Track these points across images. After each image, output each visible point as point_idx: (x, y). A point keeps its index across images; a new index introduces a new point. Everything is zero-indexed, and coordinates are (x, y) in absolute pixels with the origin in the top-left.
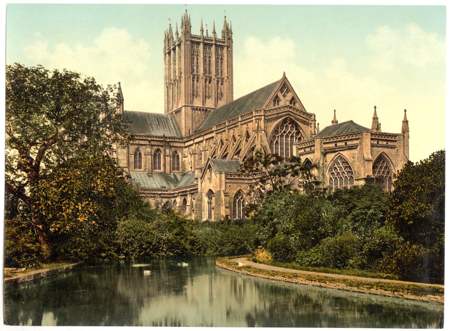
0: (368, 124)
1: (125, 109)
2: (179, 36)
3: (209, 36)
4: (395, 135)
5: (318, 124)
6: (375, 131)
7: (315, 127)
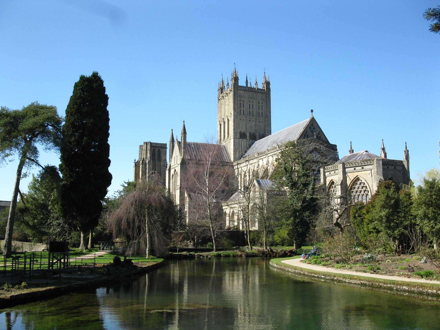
3: (252, 87)
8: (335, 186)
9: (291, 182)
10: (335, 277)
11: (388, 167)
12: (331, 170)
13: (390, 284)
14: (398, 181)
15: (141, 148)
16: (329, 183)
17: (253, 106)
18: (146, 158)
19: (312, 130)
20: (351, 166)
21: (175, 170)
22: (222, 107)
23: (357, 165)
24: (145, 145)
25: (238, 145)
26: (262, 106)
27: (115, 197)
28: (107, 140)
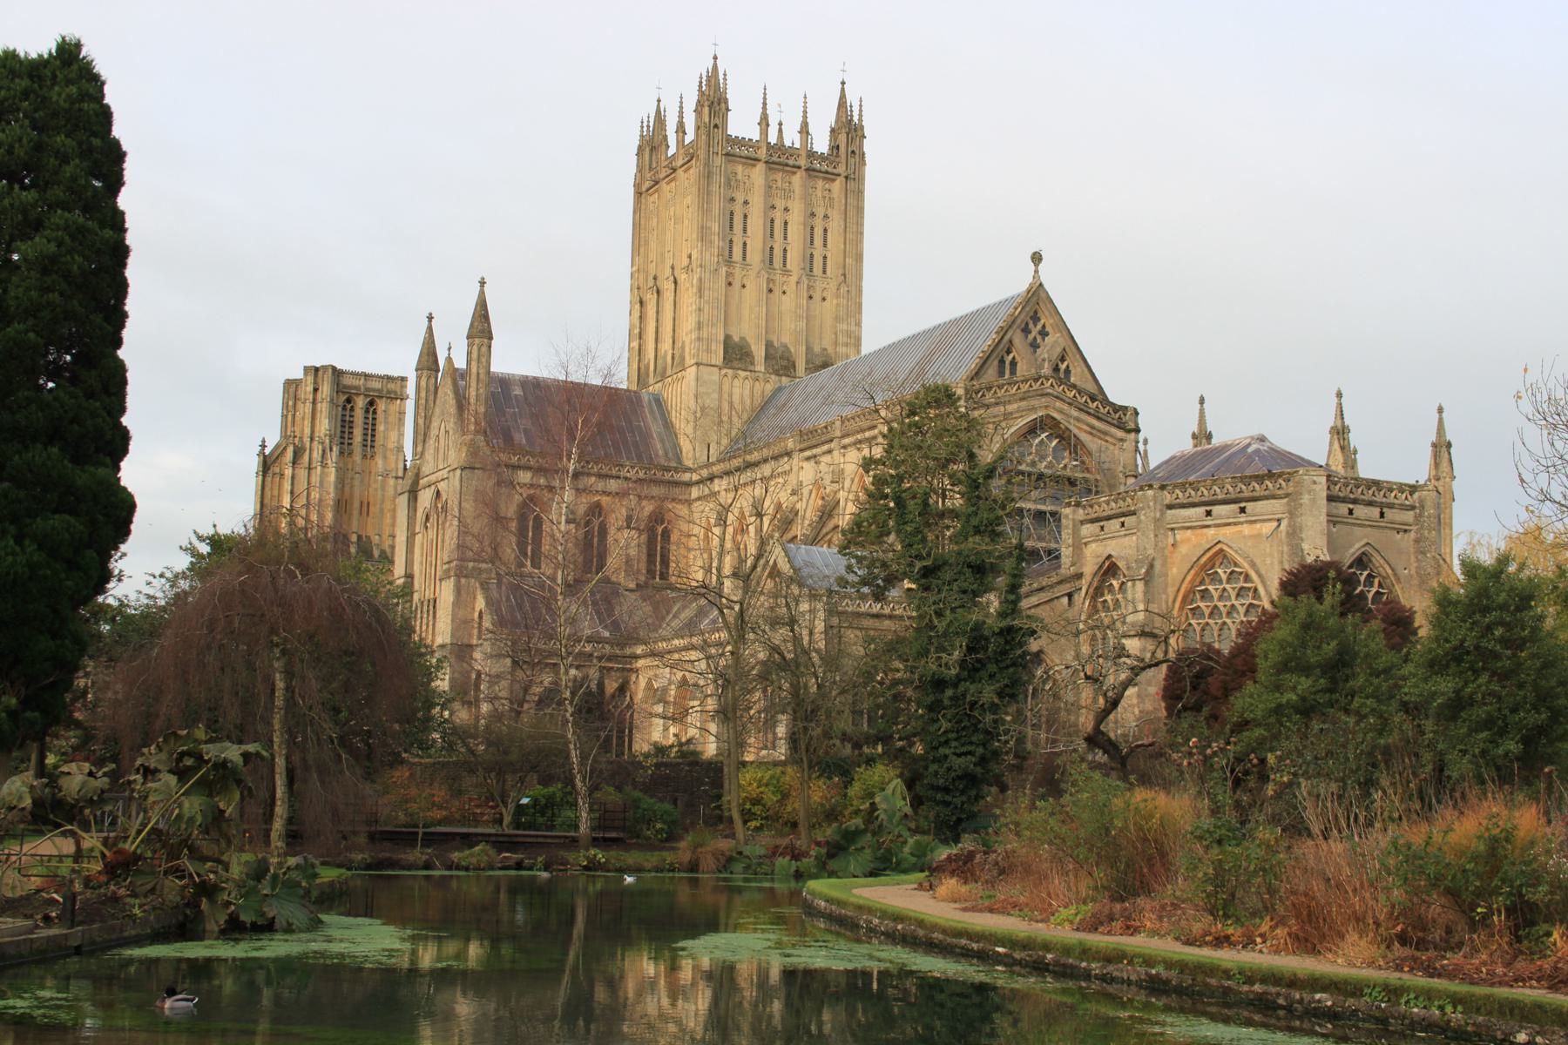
0: (1314, 446)
1: (493, 369)
2: (690, 137)
3: (788, 143)
4: (1413, 489)
5: (1146, 442)
6: (1338, 468)
7: (1137, 450)
8: (1123, 583)
9: (919, 557)
10: (1048, 950)
11: (1351, 512)
12: (1105, 514)
13: (1264, 981)
14: (1393, 570)
15: (292, 390)
16: (1096, 567)
17: (786, 229)
18: (312, 439)
19: (1035, 338)
20: (1196, 500)
21: (438, 492)
22: (655, 220)
23: (1220, 497)
24: (310, 379)
25: (715, 396)
26: (825, 230)
27: (149, 597)
28: (118, 343)
